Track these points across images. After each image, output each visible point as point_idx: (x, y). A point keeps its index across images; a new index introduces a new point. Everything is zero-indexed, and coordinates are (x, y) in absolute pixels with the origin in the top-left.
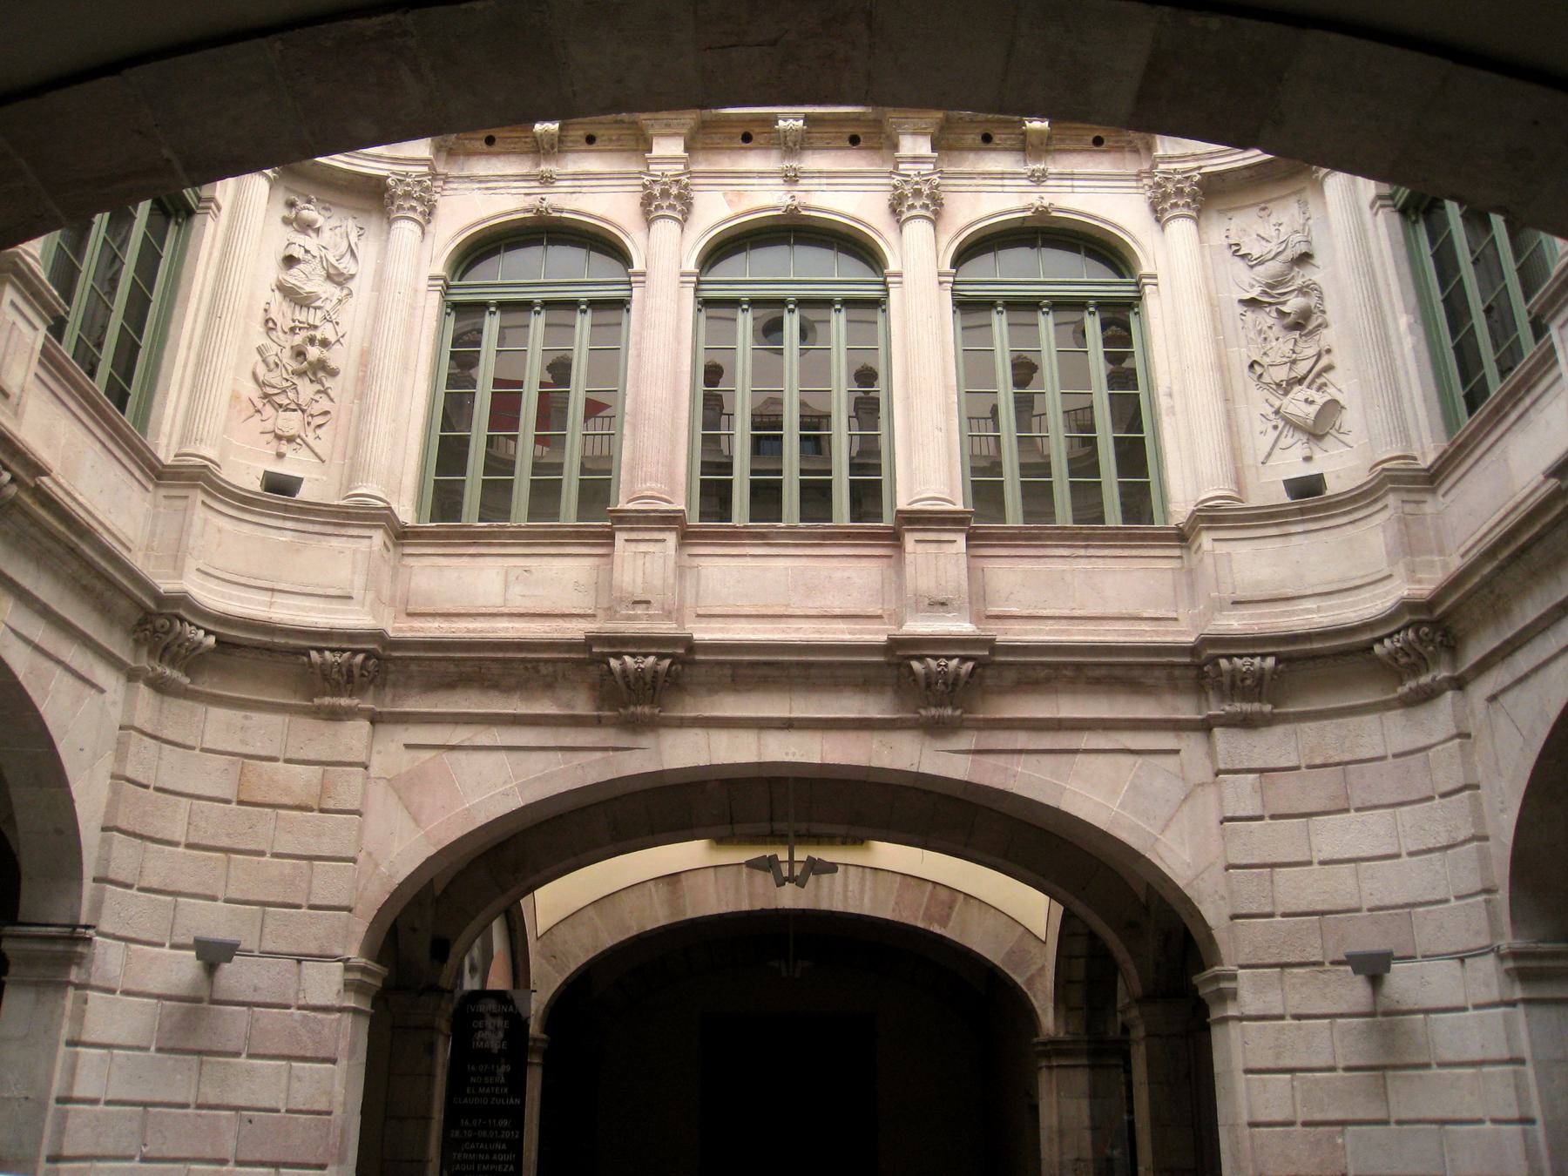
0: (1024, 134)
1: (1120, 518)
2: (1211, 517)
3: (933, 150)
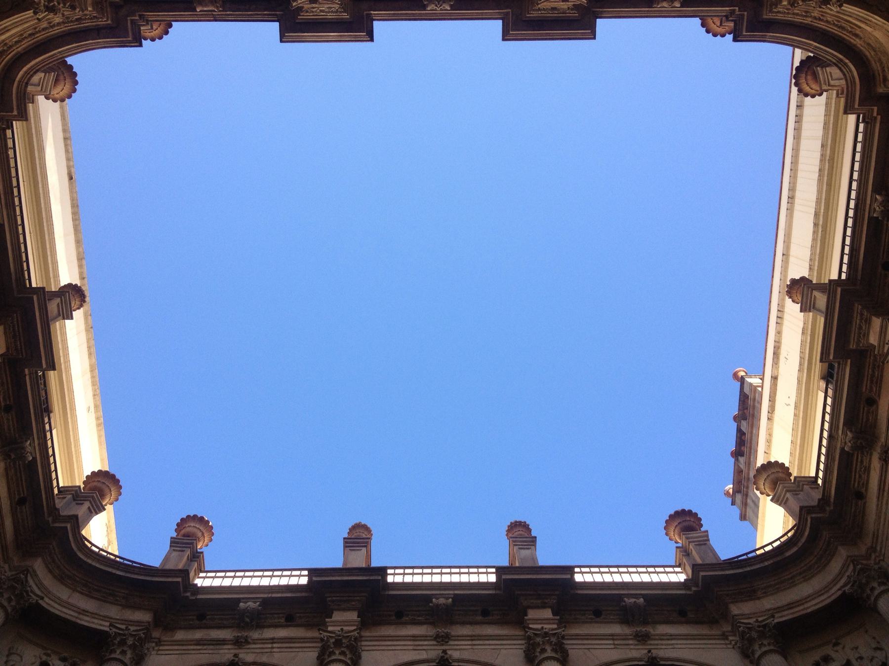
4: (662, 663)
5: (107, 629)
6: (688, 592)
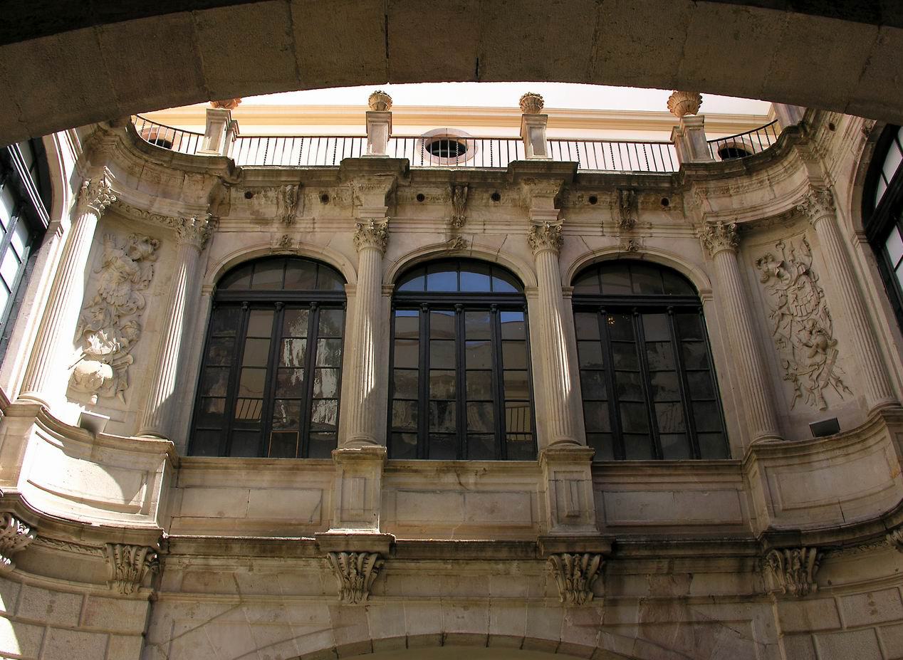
2: (761, 452)
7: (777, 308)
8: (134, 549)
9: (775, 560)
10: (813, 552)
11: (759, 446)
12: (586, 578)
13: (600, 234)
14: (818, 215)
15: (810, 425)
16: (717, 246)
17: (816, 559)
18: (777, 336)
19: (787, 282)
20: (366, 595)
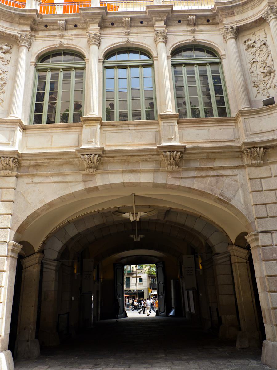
0: (188, 20)
1: (218, 116)
2: (242, 113)
3: (165, 24)
4: (197, 41)
5: (17, 34)
6: (211, 13)
7: (251, 59)
8: (8, 158)
9: (247, 152)
10: (262, 149)
11: (243, 111)
12: (175, 161)
13: (182, 35)
14: (271, 18)
15: (263, 101)
16: (228, 37)
17: (263, 152)
18: (251, 71)
19: (256, 49)
20: (95, 170)
